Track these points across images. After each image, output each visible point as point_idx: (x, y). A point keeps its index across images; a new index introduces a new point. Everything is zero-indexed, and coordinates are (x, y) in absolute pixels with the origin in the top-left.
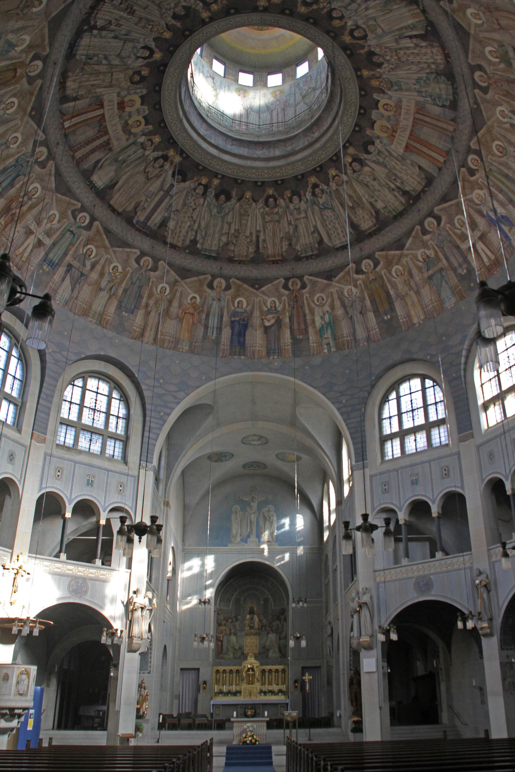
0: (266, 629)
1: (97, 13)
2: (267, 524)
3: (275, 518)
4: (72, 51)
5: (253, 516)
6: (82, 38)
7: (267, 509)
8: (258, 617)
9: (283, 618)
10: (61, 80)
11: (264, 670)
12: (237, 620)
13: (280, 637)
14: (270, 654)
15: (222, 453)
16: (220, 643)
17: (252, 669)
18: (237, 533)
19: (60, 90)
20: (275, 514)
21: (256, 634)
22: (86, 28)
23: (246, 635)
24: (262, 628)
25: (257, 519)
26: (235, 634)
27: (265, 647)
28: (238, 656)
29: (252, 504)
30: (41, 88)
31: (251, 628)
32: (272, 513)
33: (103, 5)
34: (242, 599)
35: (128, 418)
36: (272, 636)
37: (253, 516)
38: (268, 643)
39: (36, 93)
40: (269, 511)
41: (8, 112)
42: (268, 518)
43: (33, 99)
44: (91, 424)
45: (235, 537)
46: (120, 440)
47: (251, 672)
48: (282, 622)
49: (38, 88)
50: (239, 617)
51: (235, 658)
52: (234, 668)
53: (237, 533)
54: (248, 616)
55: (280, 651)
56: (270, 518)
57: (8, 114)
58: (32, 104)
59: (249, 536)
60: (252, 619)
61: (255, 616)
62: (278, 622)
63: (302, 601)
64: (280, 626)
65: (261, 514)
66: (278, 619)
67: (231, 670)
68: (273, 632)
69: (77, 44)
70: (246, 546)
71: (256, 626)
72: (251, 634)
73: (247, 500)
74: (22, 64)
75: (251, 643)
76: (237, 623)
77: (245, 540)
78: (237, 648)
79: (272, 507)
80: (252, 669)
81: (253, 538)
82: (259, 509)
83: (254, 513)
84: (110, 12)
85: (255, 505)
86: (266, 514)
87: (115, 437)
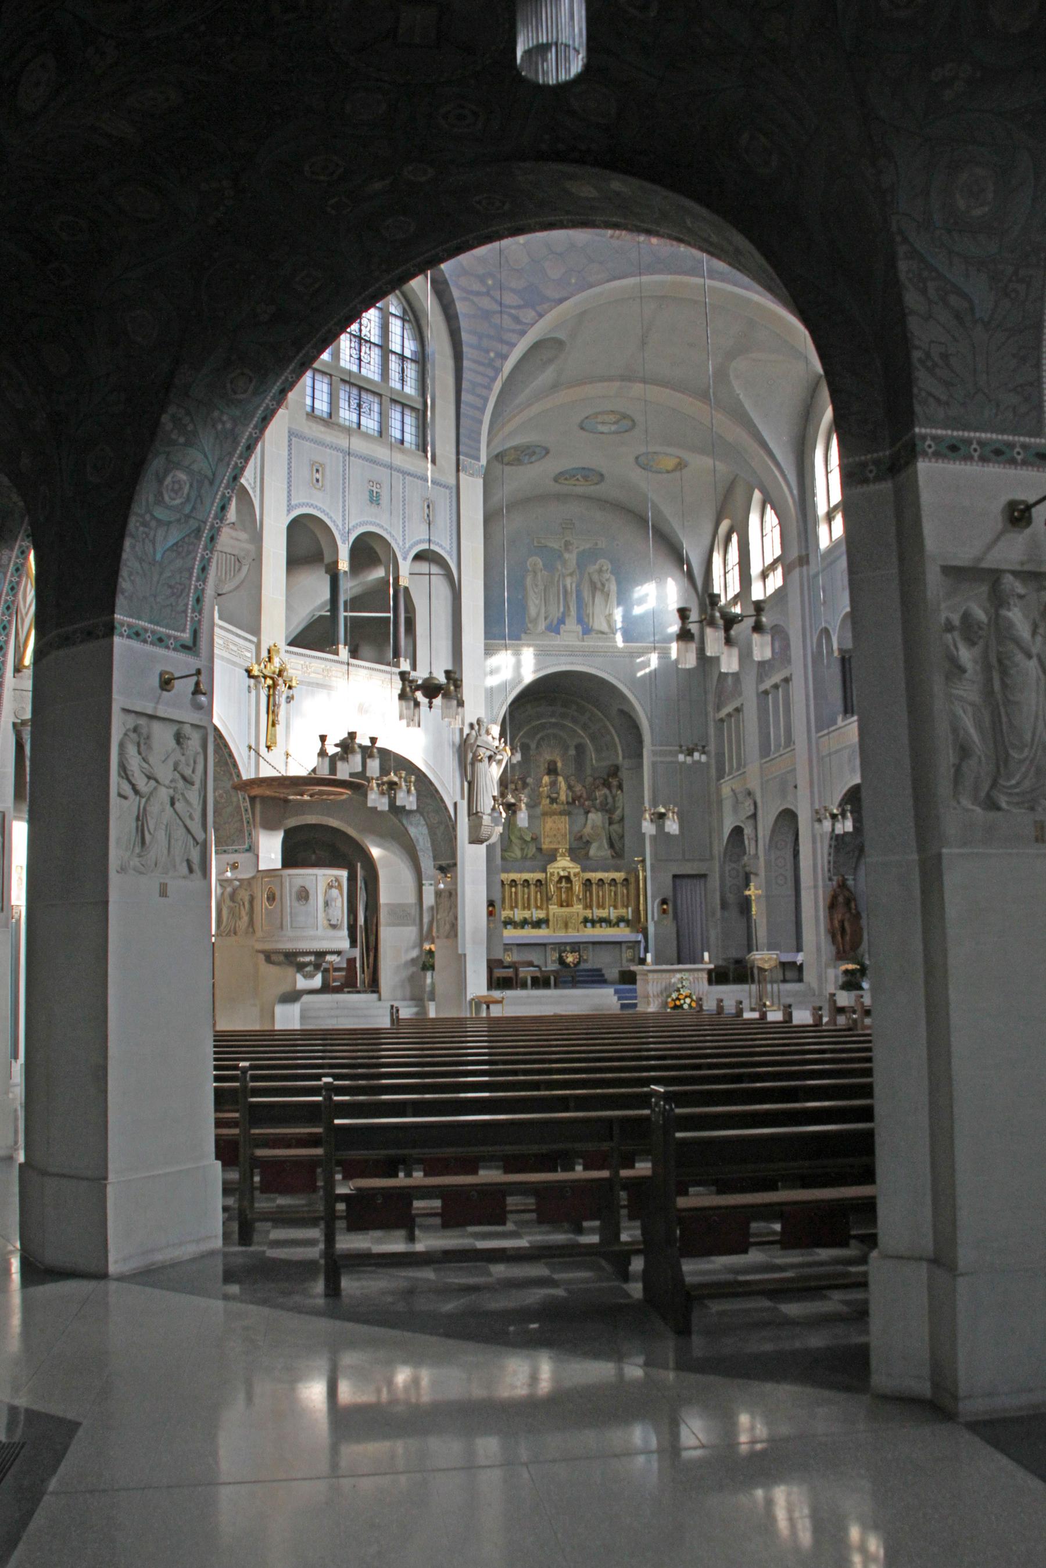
0: (582, 805)
2: (599, 598)
3: (613, 587)
5: (568, 581)
7: (597, 567)
8: (566, 779)
11: (589, 880)
12: (525, 785)
13: (610, 818)
15: (528, 447)
17: (568, 879)
18: (538, 614)
20: (613, 578)
21: (562, 813)
23: (545, 814)
24: (574, 801)
25: (578, 585)
27: (581, 837)
28: (530, 855)
29: (567, 556)
31: (553, 801)
32: (607, 575)
34: (533, 746)
35: (421, 360)
36: (596, 818)
37: (568, 581)
38: (588, 830)
40: (600, 571)
42: (599, 585)
44: (355, 369)
45: (535, 621)
46: (413, 409)
47: (564, 884)
48: (614, 790)
50: (529, 780)
51: (524, 858)
53: (538, 614)
54: (546, 779)
55: (612, 845)
56: (603, 585)
59: (562, 621)
60: (553, 784)
61: (560, 779)
62: (606, 791)
63: (698, 751)
64: (610, 800)
65: (586, 575)
66: (607, 785)
68: (597, 810)
70: (557, 641)
71: (563, 797)
72: (554, 813)
73: (556, 546)
75: (556, 829)
77: (554, 629)
78: (528, 839)
79: (607, 566)
80: (568, 879)
81: (572, 625)
82: (581, 566)
83: (571, 574)
85: (571, 558)
86: (595, 577)
87: (401, 403)
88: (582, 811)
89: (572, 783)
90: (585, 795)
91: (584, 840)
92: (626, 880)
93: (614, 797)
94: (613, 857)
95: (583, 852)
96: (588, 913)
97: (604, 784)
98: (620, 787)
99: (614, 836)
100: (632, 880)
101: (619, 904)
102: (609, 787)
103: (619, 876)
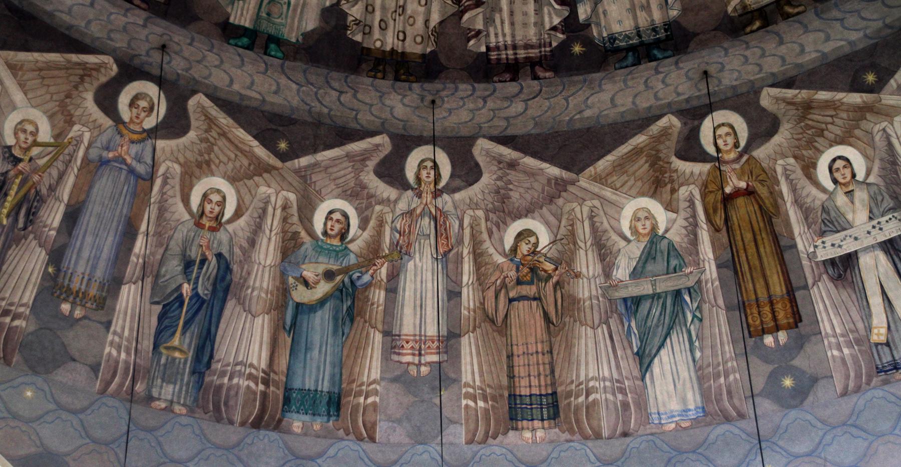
1: (527, 46)
4: (657, 43)
6: (612, 38)
10: (757, 24)
19: (787, 16)
22: (577, 49)
30: (789, 84)
33: (497, 48)
39: (803, 94)
41: (860, 176)
43: (823, 95)
49: (789, 93)
57: (868, 174)
58: (840, 95)
69: (635, 41)
74: (711, 187)
84: (512, 13)
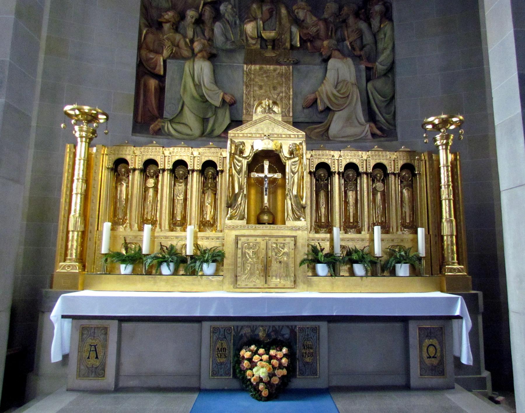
0: (318, 50)
9: (378, 8)
11: (323, 166)
12: (217, 16)
13: (368, 69)
14: (336, 126)
16: (153, 83)
26: (212, 57)
36: (342, 69)
52: (194, 156)
55: (371, 116)
64: (368, 38)
67: (180, 163)
68: (344, 55)
72: (269, 61)
76: (218, 28)
78: (217, 103)
88: (318, 60)
89: (301, 15)
90: (322, 33)
91: (321, 107)
92: (408, 167)
93: (375, 35)
94: (374, 135)
95: (319, 129)
96: (321, 239)
97: (357, 15)
98: (387, 15)
99: (377, 99)
100: (422, 168)
101: (393, 223)
102: (368, 20)
103: (393, 160)
